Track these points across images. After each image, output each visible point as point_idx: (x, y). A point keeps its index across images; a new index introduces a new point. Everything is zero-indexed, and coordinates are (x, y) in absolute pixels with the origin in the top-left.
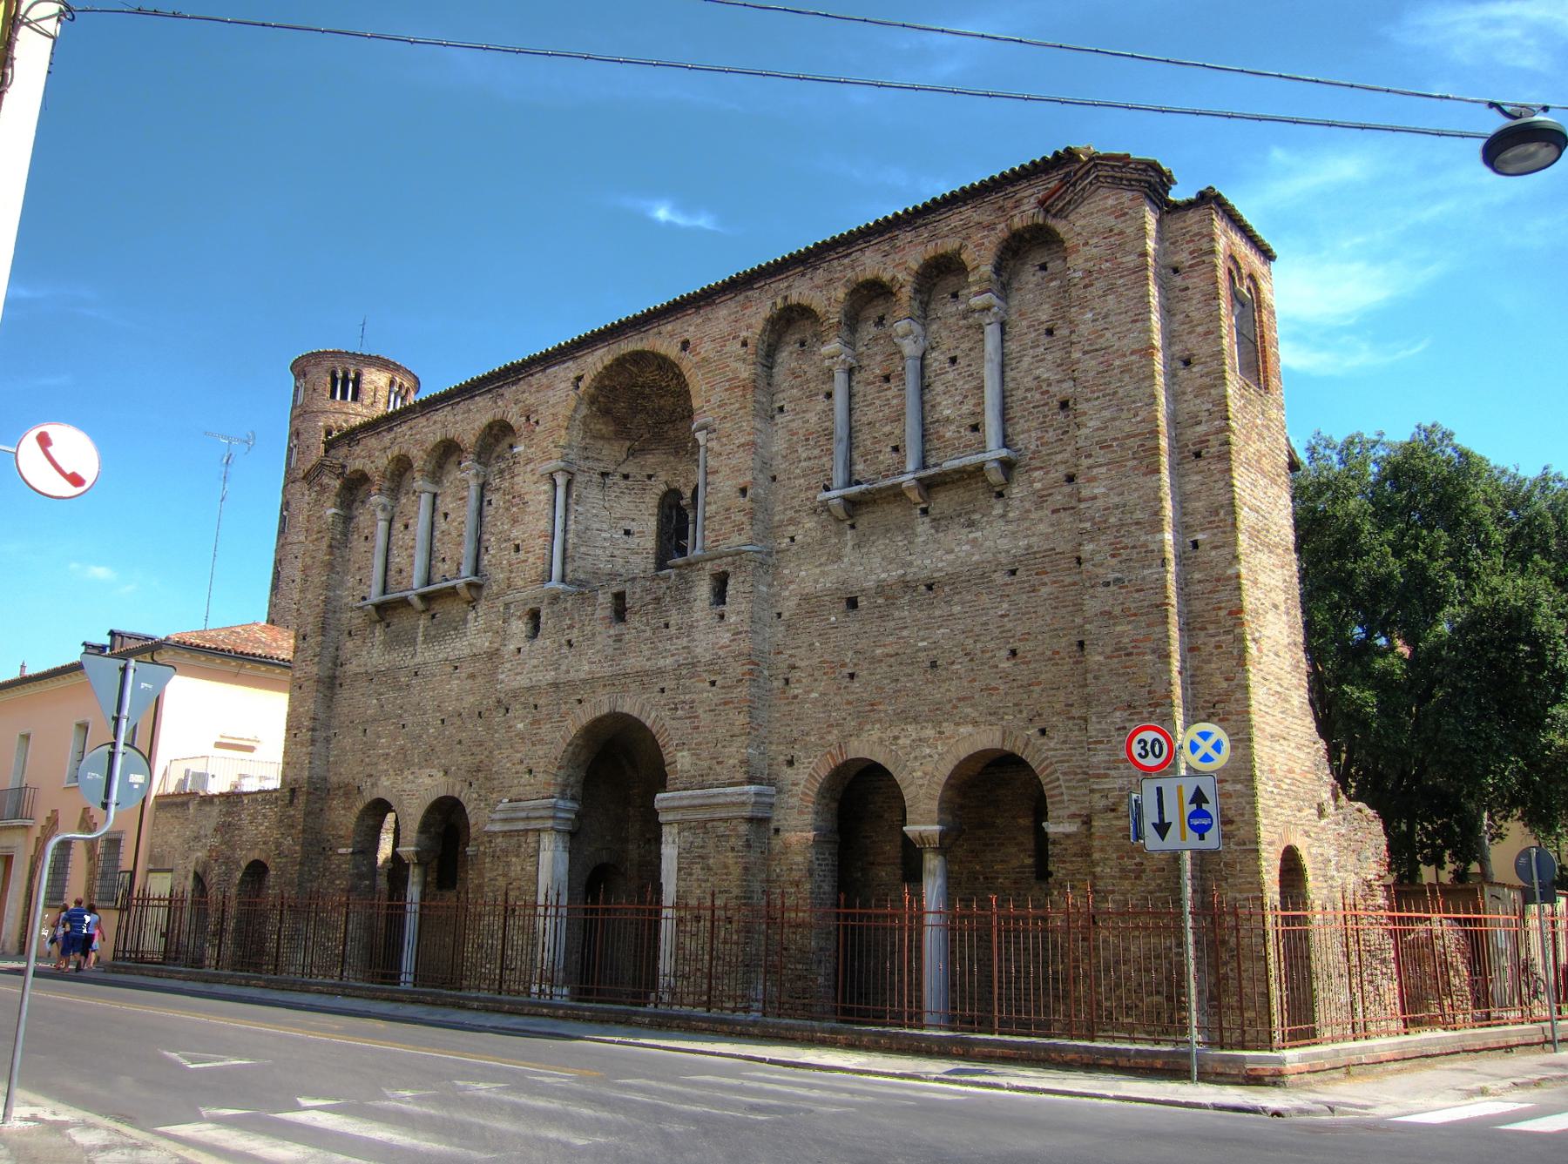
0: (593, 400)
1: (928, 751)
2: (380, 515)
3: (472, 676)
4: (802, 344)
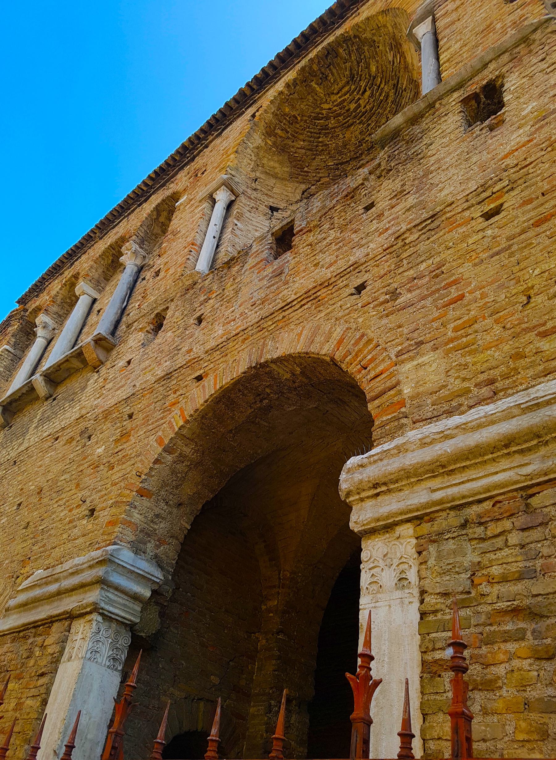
0: (269, 132)
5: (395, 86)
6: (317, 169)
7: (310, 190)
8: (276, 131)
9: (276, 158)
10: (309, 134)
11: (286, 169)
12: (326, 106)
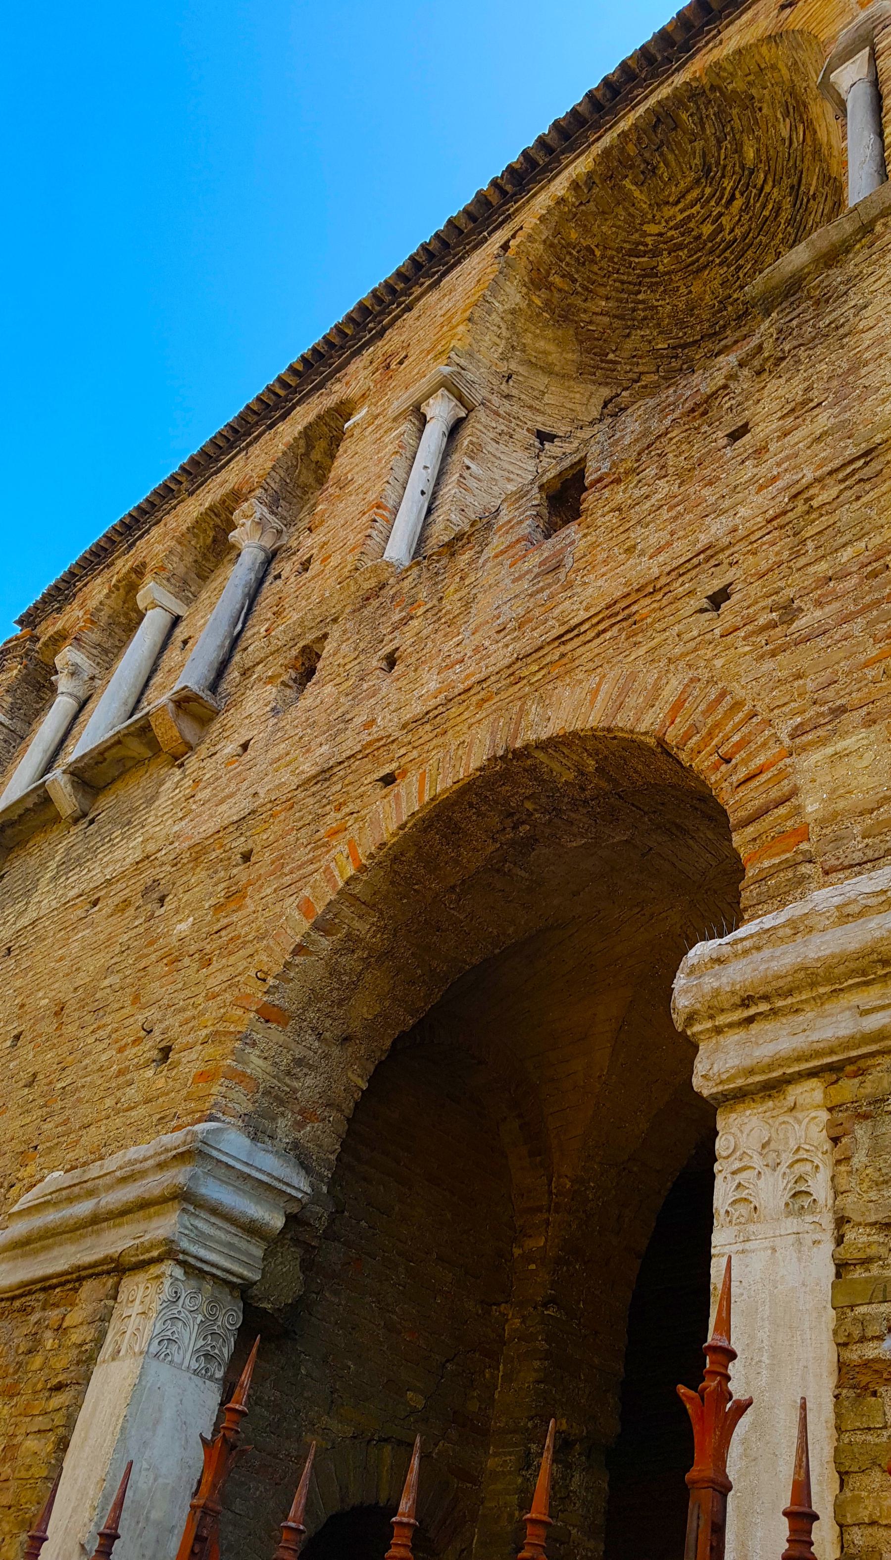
5: (795, 189)
6: (634, 357)
7: (619, 399)
8: (551, 279)
9: (549, 333)
10: (617, 284)
11: (570, 356)
12: (653, 229)
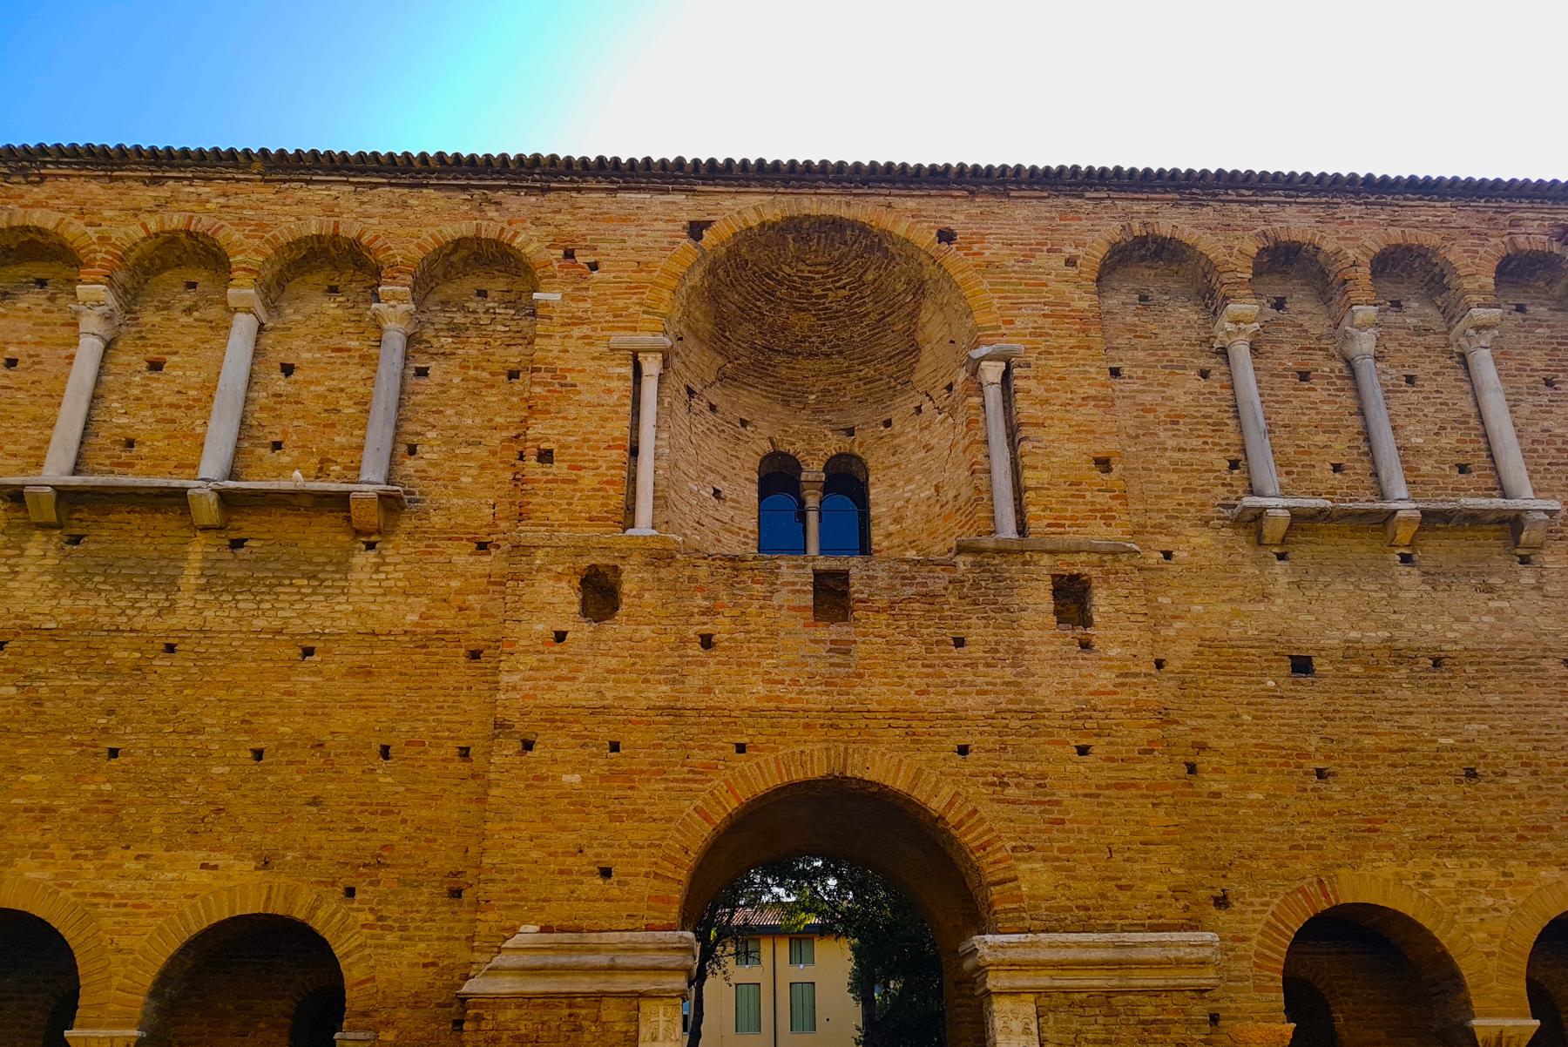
0: (711, 272)
1: (1490, 901)
2: (91, 322)
3: (366, 672)
4: (1143, 298)
12: (787, 269)
